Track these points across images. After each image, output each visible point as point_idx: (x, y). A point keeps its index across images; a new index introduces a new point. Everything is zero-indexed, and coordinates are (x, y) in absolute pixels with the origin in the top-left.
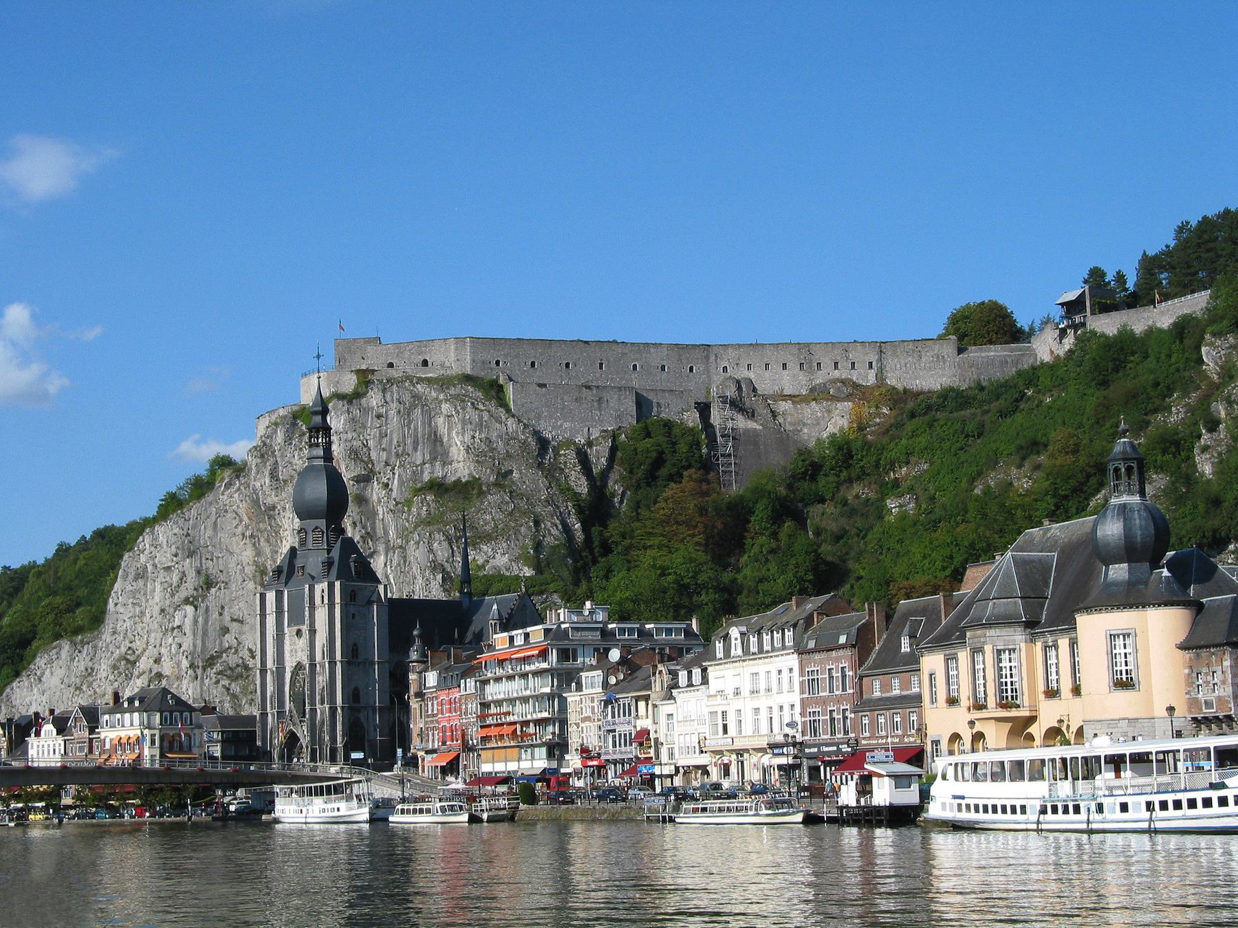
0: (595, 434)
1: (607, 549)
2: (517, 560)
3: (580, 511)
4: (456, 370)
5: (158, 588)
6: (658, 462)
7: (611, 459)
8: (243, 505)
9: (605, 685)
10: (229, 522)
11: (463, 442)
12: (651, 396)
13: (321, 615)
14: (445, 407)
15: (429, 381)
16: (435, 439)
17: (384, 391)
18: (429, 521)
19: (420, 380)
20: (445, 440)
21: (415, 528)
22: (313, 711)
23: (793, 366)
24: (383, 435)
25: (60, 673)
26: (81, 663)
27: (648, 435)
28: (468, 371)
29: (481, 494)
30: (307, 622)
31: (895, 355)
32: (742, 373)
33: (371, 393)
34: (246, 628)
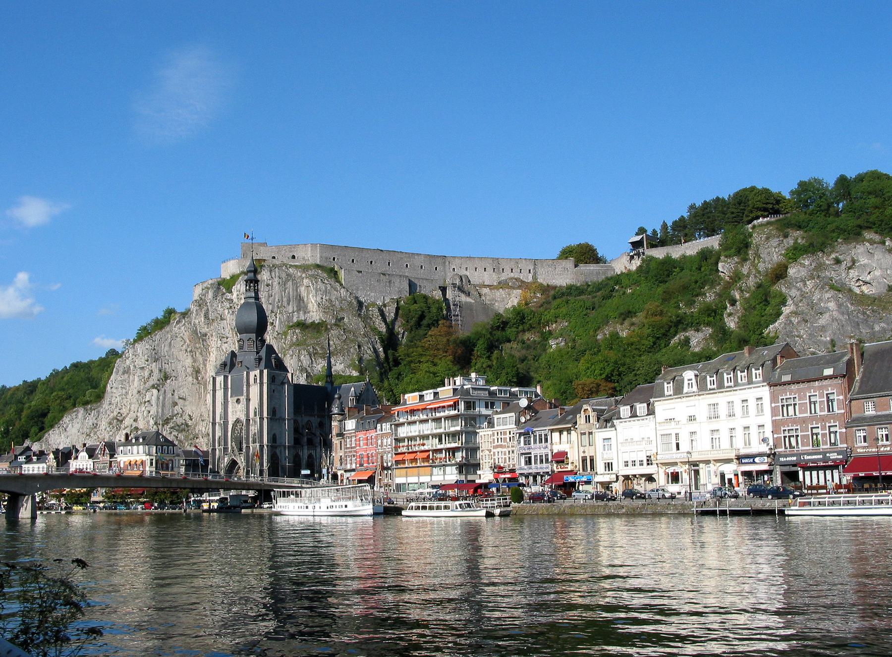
0: (387, 300)
1: (397, 363)
2: (349, 367)
3: (382, 341)
4: (311, 261)
5: (136, 379)
6: (422, 317)
7: (397, 314)
8: (187, 334)
9: (518, 422)
10: (178, 343)
11: (316, 301)
12: (416, 281)
13: (254, 390)
14: (306, 281)
15: (296, 267)
16: (300, 299)
17: (271, 271)
18: (298, 344)
19: (291, 266)
20: (305, 299)
21: (290, 347)
22: (248, 447)
23: (490, 270)
24: (270, 296)
25: (77, 426)
26: (90, 420)
27: (415, 302)
28: (318, 263)
29: (327, 329)
30: (245, 394)
31: (542, 266)
32: (463, 272)
33: (263, 272)
34: (187, 403)
